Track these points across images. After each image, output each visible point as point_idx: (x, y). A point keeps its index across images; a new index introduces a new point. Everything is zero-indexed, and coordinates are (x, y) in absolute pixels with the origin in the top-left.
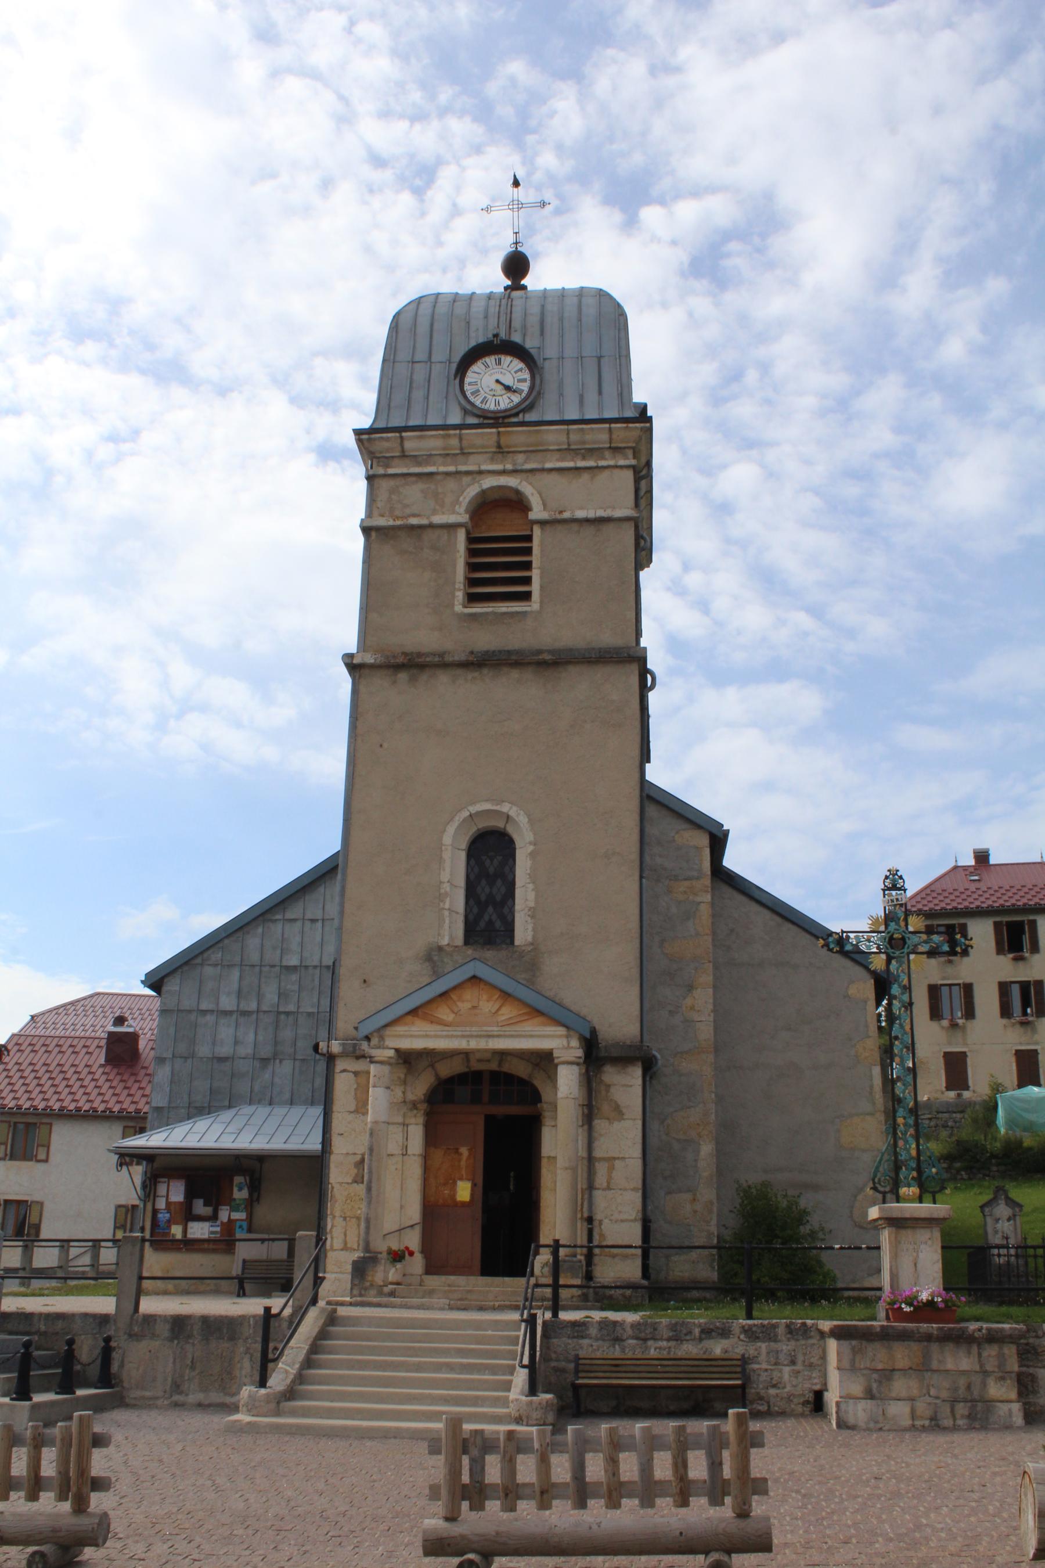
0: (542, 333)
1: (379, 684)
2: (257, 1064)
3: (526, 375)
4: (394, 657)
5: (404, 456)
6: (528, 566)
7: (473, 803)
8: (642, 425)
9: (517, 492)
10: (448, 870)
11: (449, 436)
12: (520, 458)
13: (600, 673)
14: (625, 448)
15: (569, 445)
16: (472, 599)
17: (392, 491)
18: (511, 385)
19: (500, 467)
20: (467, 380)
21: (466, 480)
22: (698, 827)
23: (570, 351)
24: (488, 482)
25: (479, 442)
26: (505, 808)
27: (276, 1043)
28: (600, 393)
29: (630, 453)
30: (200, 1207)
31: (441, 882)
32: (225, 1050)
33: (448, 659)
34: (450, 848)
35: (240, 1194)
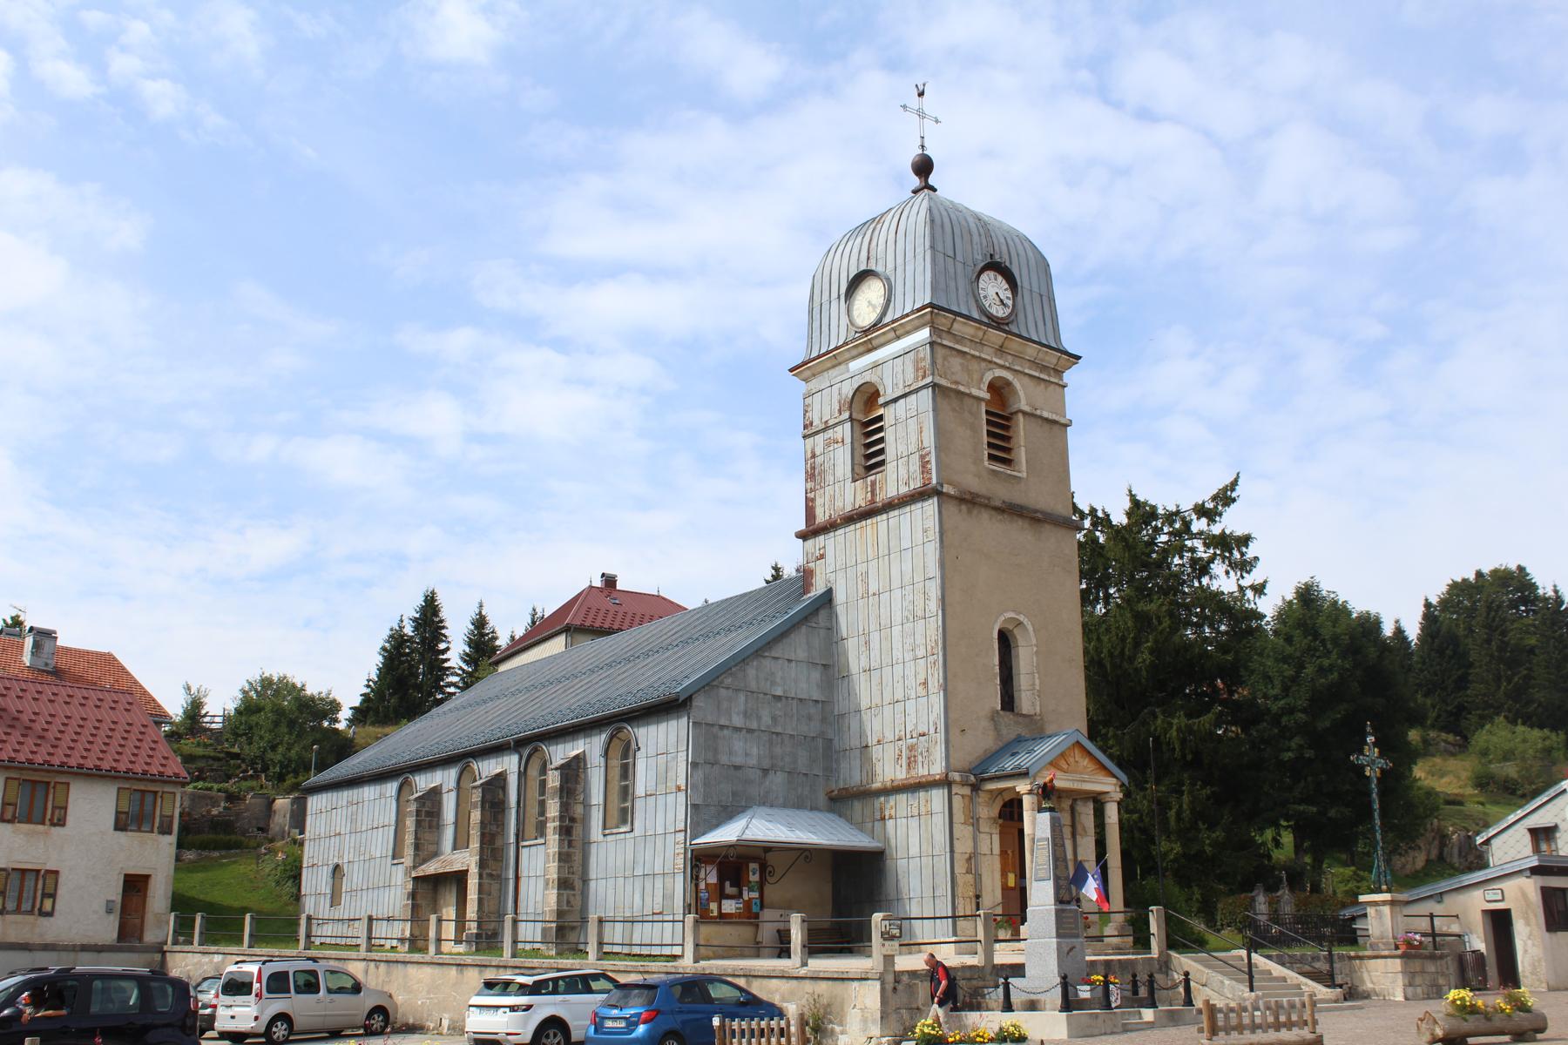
5: (949, 332)
24: (999, 373)
25: (993, 339)
26: (1021, 618)
30: (729, 889)
32: (738, 760)
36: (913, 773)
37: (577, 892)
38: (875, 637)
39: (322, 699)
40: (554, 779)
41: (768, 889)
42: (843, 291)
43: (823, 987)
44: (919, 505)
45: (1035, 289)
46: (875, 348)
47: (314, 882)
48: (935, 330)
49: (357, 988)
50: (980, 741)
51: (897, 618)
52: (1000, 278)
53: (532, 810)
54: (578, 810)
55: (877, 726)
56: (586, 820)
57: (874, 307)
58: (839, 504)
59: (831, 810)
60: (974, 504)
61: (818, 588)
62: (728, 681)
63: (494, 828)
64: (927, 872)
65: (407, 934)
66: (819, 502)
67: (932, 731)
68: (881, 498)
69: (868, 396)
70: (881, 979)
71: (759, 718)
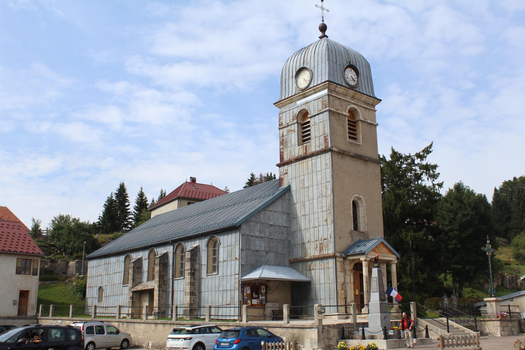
2: (265, 253)
5: (334, 91)
25: (350, 94)
26: (361, 196)
27: (269, 247)
30: (255, 296)
32: (258, 248)
35: (263, 291)
36: (322, 253)
37: (197, 297)
38: (307, 203)
39: (86, 224)
40: (188, 255)
41: (268, 295)
42: (294, 74)
43: (296, 331)
44: (324, 155)
45: (365, 74)
46: (307, 96)
47: (91, 293)
48: (329, 90)
49: (118, 332)
50: (346, 242)
51: (316, 196)
52: (353, 71)
53: (178, 266)
54: (197, 266)
55: (308, 236)
56: (200, 270)
57: (306, 81)
58: (293, 154)
59: (290, 267)
60: (344, 154)
61: (285, 185)
62: (254, 219)
63: (164, 273)
64: (327, 289)
65: (130, 312)
66: (285, 153)
67: (329, 238)
68: (309, 152)
69: (304, 114)
70: (318, 328)
71: (265, 233)
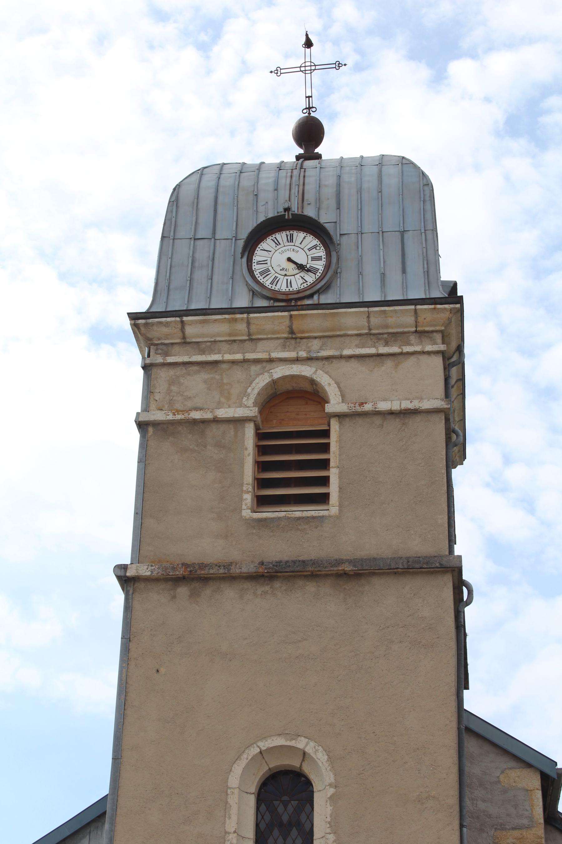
0: (338, 208)
1: (155, 599)
3: (321, 252)
4: (174, 568)
5: (185, 342)
6: (325, 464)
7: (264, 738)
8: (452, 306)
9: (312, 382)
10: (234, 818)
11: (236, 320)
12: (315, 344)
13: (408, 586)
14: (432, 332)
15: (370, 329)
16: (262, 502)
17: (172, 382)
18: (304, 263)
19: (293, 355)
20: (256, 259)
21: (254, 369)
22: (529, 765)
23: (369, 226)
24: (280, 372)
26: (301, 743)
28: (404, 271)
29: (438, 337)
31: (226, 833)
33: (235, 570)
34: (236, 791)
